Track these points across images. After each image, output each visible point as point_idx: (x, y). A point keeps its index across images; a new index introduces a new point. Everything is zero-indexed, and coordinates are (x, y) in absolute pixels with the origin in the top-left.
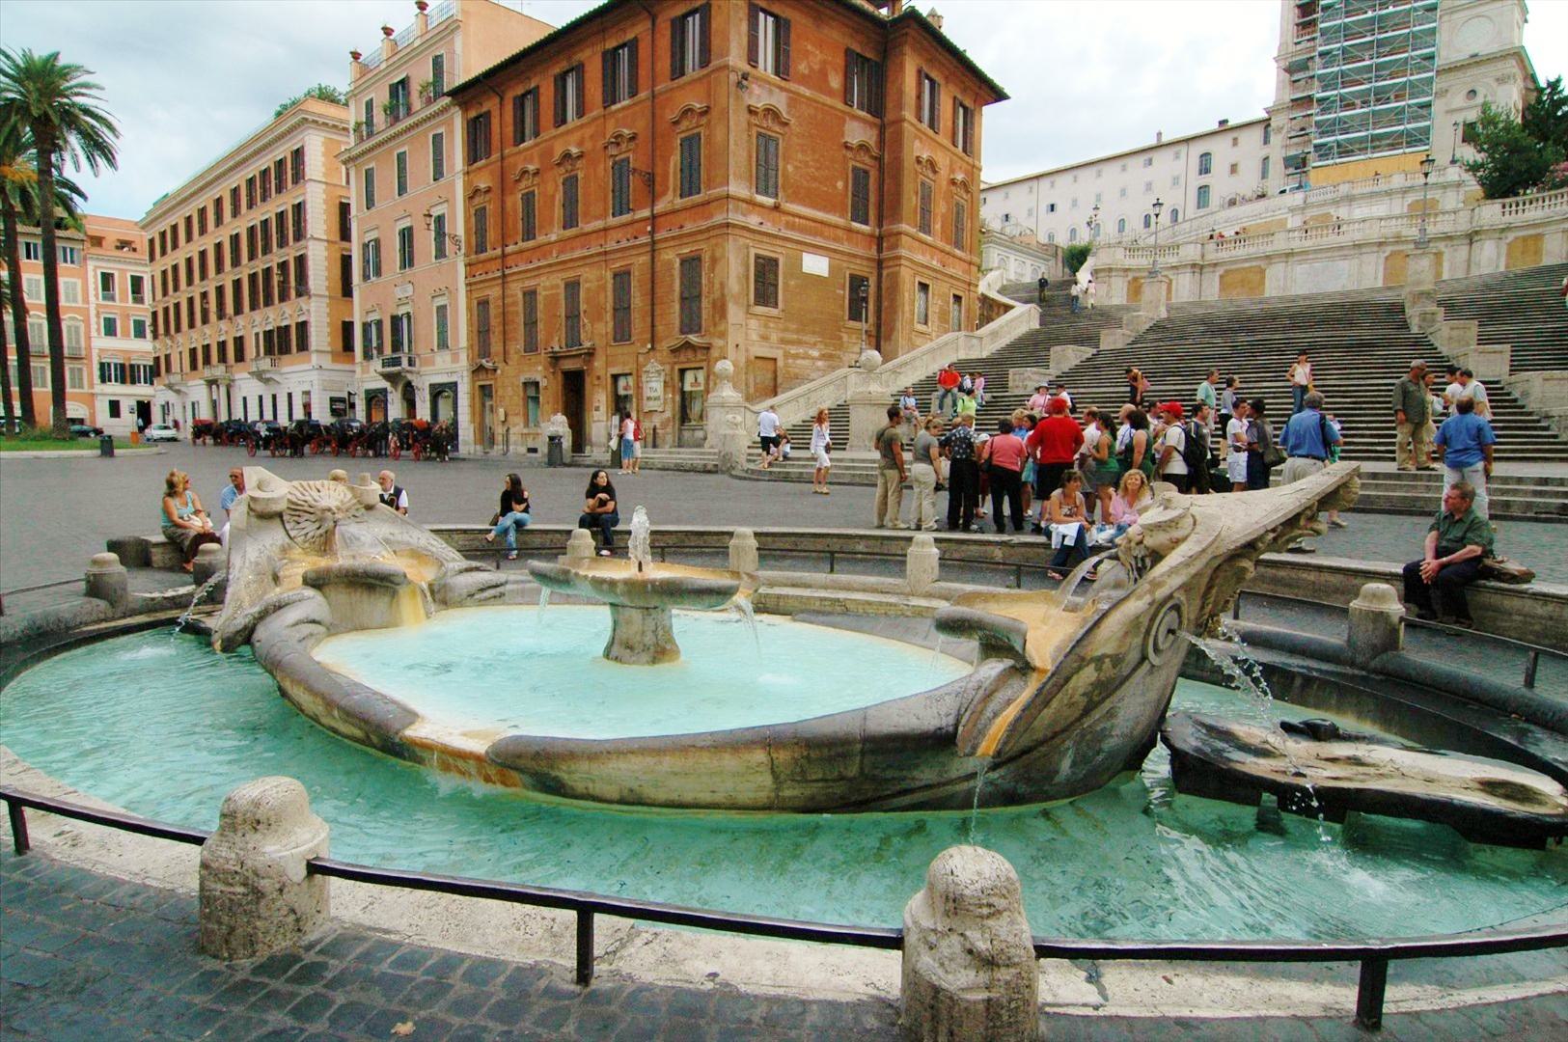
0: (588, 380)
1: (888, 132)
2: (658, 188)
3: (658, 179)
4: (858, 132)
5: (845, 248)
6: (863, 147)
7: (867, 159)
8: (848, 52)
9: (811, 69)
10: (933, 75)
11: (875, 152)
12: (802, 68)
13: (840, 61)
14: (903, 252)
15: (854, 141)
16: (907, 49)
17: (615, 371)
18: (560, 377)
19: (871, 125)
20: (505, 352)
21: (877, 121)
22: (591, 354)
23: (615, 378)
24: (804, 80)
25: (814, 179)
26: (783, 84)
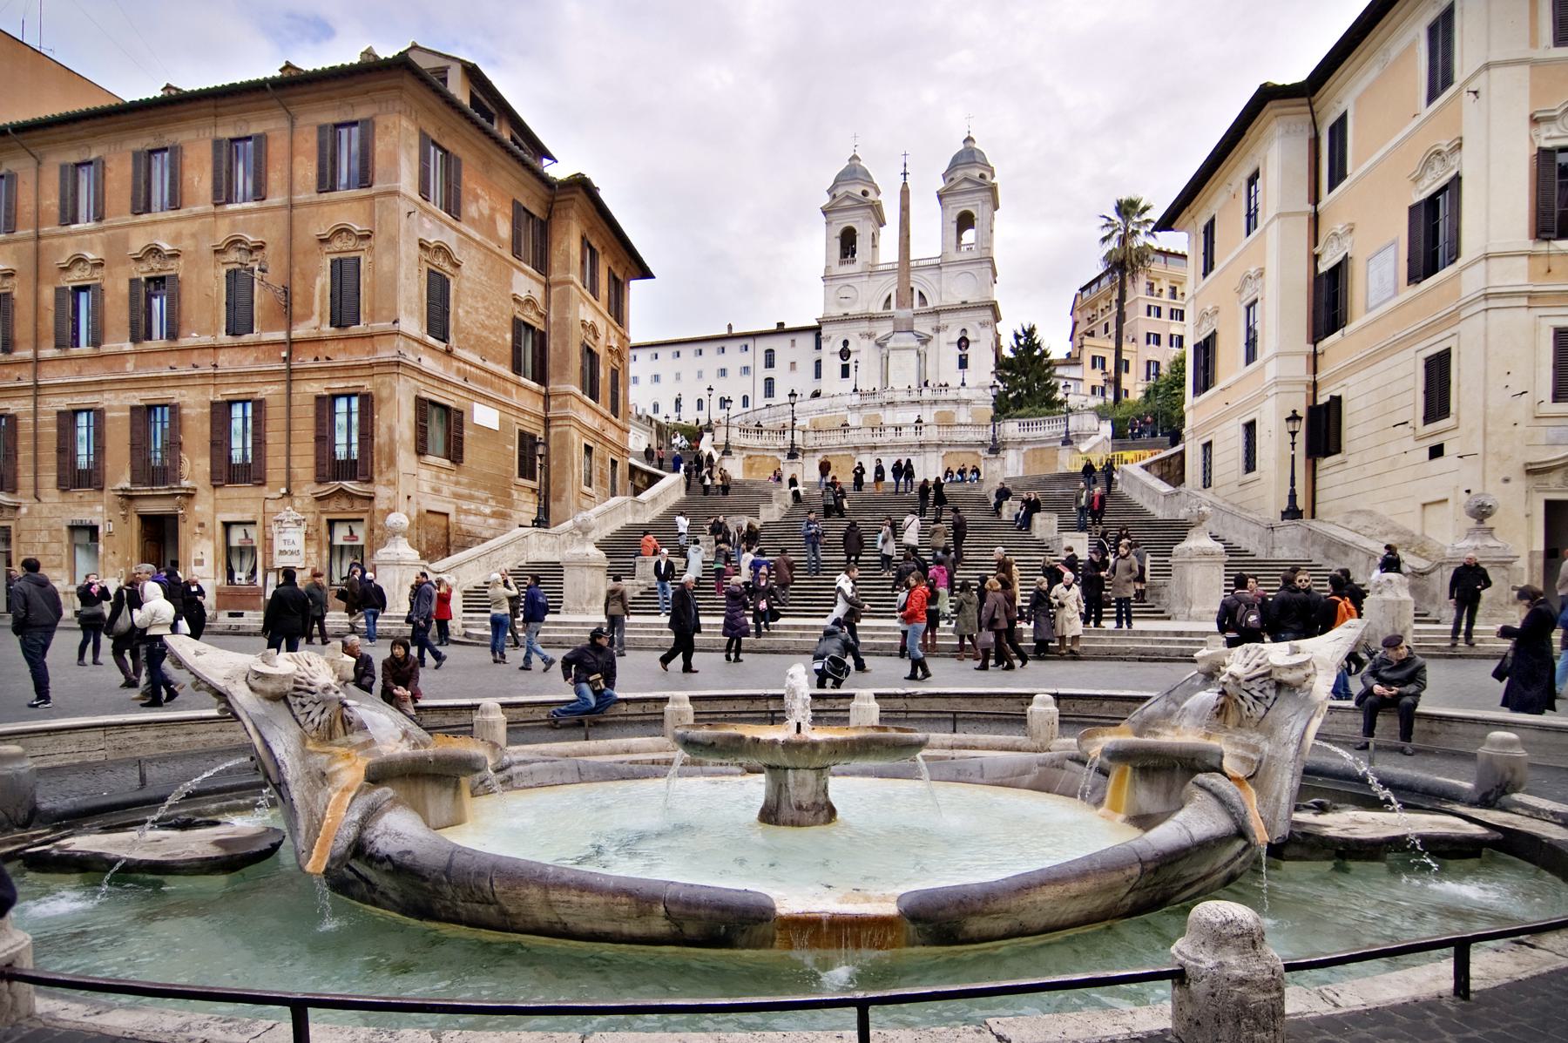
0: (183, 529)
1: (554, 291)
2: (297, 309)
3: (297, 299)
4: (525, 284)
5: (515, 401)
6: (530, 302)
7: (533, 315)
8: (515, 203)
9: (481, 214)
10: (594, 243)
11: (541, 308)
12: (471, 209)
13: (509, 211)
14: (572, 413)
15: (523, 295)
16: (573, 214)
17: (229, 518)
18: (135, 522)
19: (538, 281)
20: (36, 487)
21: (543, 279)
22: (190, 495)
23: (227, 526)
24: (473, 222)
25: (484, 327)
26: (454, 223)
